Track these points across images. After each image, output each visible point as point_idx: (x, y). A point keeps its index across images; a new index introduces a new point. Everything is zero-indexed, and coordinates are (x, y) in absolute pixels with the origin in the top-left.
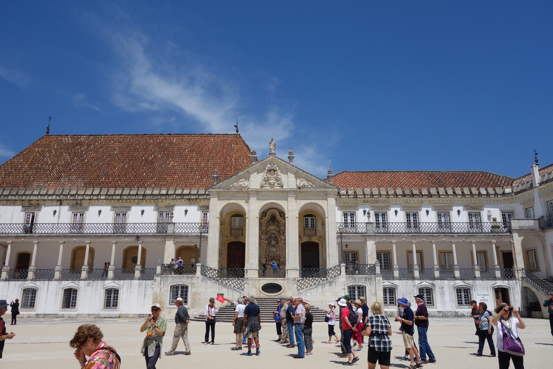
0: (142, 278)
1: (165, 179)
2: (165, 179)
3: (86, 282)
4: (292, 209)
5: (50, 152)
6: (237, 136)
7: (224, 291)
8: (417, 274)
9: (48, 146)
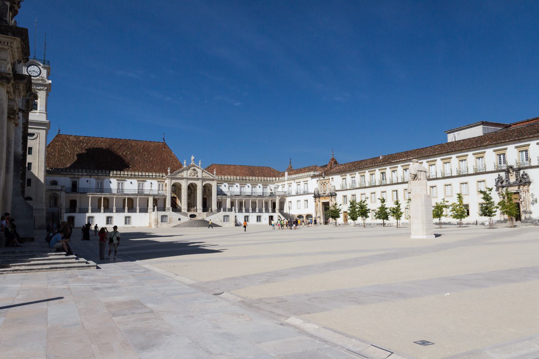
0: (140, 212)
1: (135, 166)
2: (135, 166)
3: (117, 214)
4: (200, 185)
5: (66, 145)
6: (165, 144)
7: (181, 216)
8: (244, 211)
9: (63, 141)
